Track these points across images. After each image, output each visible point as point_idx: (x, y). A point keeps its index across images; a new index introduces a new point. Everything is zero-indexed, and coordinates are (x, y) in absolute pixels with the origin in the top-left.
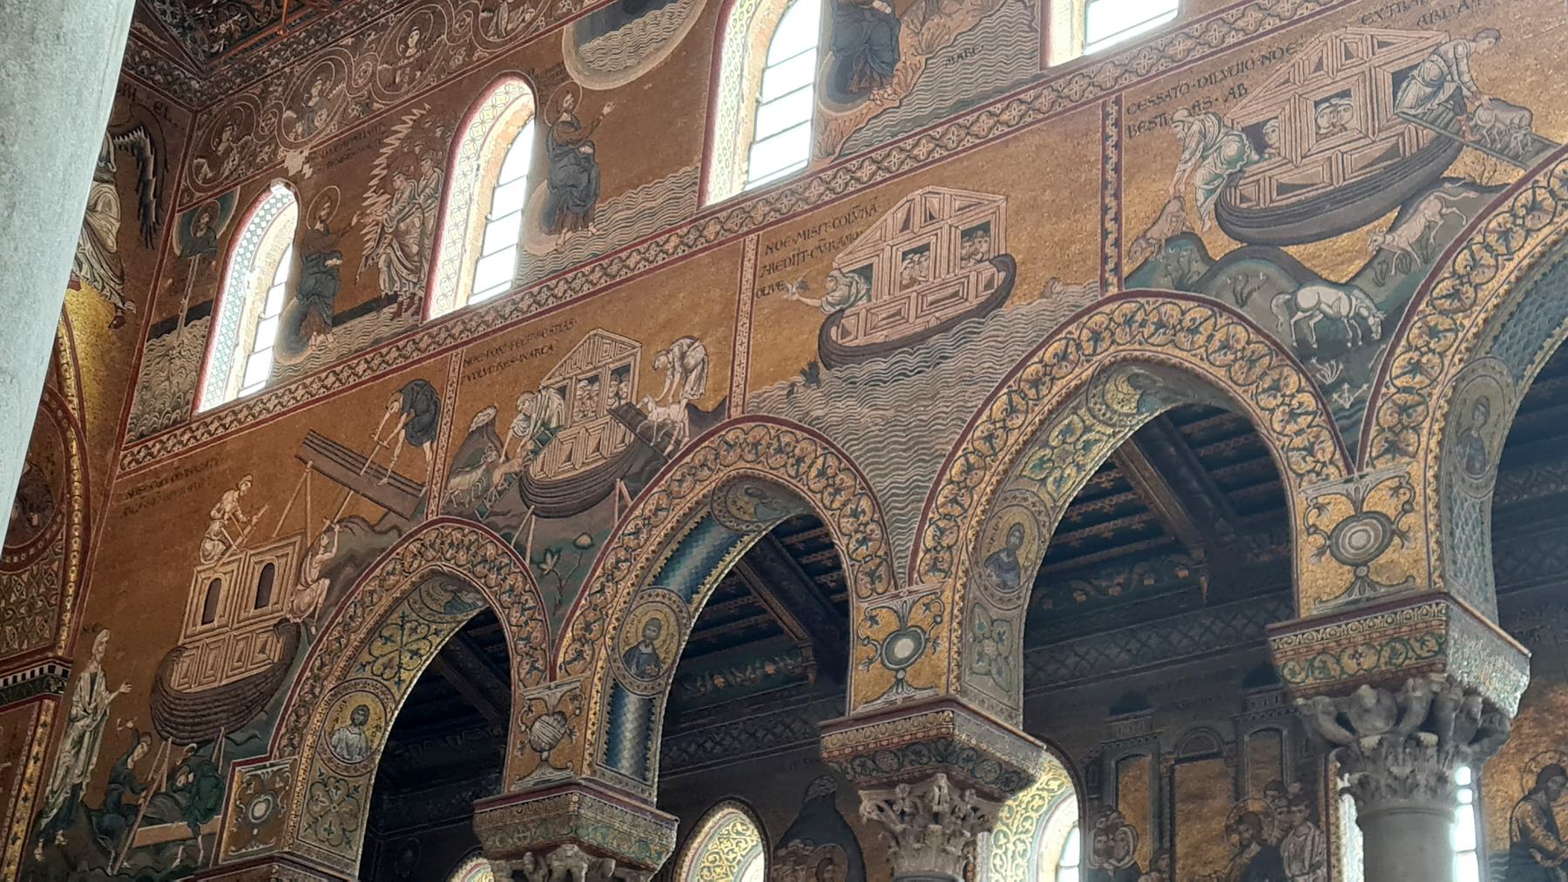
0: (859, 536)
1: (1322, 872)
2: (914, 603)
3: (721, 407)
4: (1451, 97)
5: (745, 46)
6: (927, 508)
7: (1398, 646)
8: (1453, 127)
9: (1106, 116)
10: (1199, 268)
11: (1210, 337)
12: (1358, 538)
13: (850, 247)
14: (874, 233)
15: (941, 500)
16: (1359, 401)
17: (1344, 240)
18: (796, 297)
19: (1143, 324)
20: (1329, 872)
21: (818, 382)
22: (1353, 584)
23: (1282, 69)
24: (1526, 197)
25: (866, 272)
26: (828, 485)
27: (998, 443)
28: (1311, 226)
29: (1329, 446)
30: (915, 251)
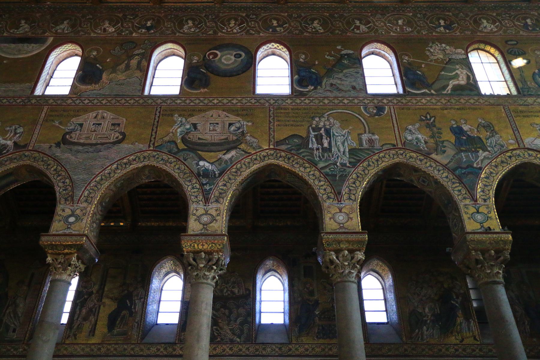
0: (64, 188)
1: (142, 300)
2: (77, 209)
3: (25, 146)
4: (241, 132)
5: (52, 62)
6: (87, 186)
7: (213, 245)
8: (241, 138)
9: (157, 110)
10: (175, 150)
11: (175, 166)
12: (205, 219)
13: (77, 118)
14: (86, 116)
15: (91, 185)
16: (211, 189)
17: (212, 154)
18: (57, 125)
19: (158, 158)
20: (144, 300)
21: (60, 147)
22: (202, 229)
23: (203, 114)
24: (255, 157)
25: (81, 125)
26: (56, 173)
27: (112, 175)
28: (206, 148)
29: (201, 197)
30: (97, 124)
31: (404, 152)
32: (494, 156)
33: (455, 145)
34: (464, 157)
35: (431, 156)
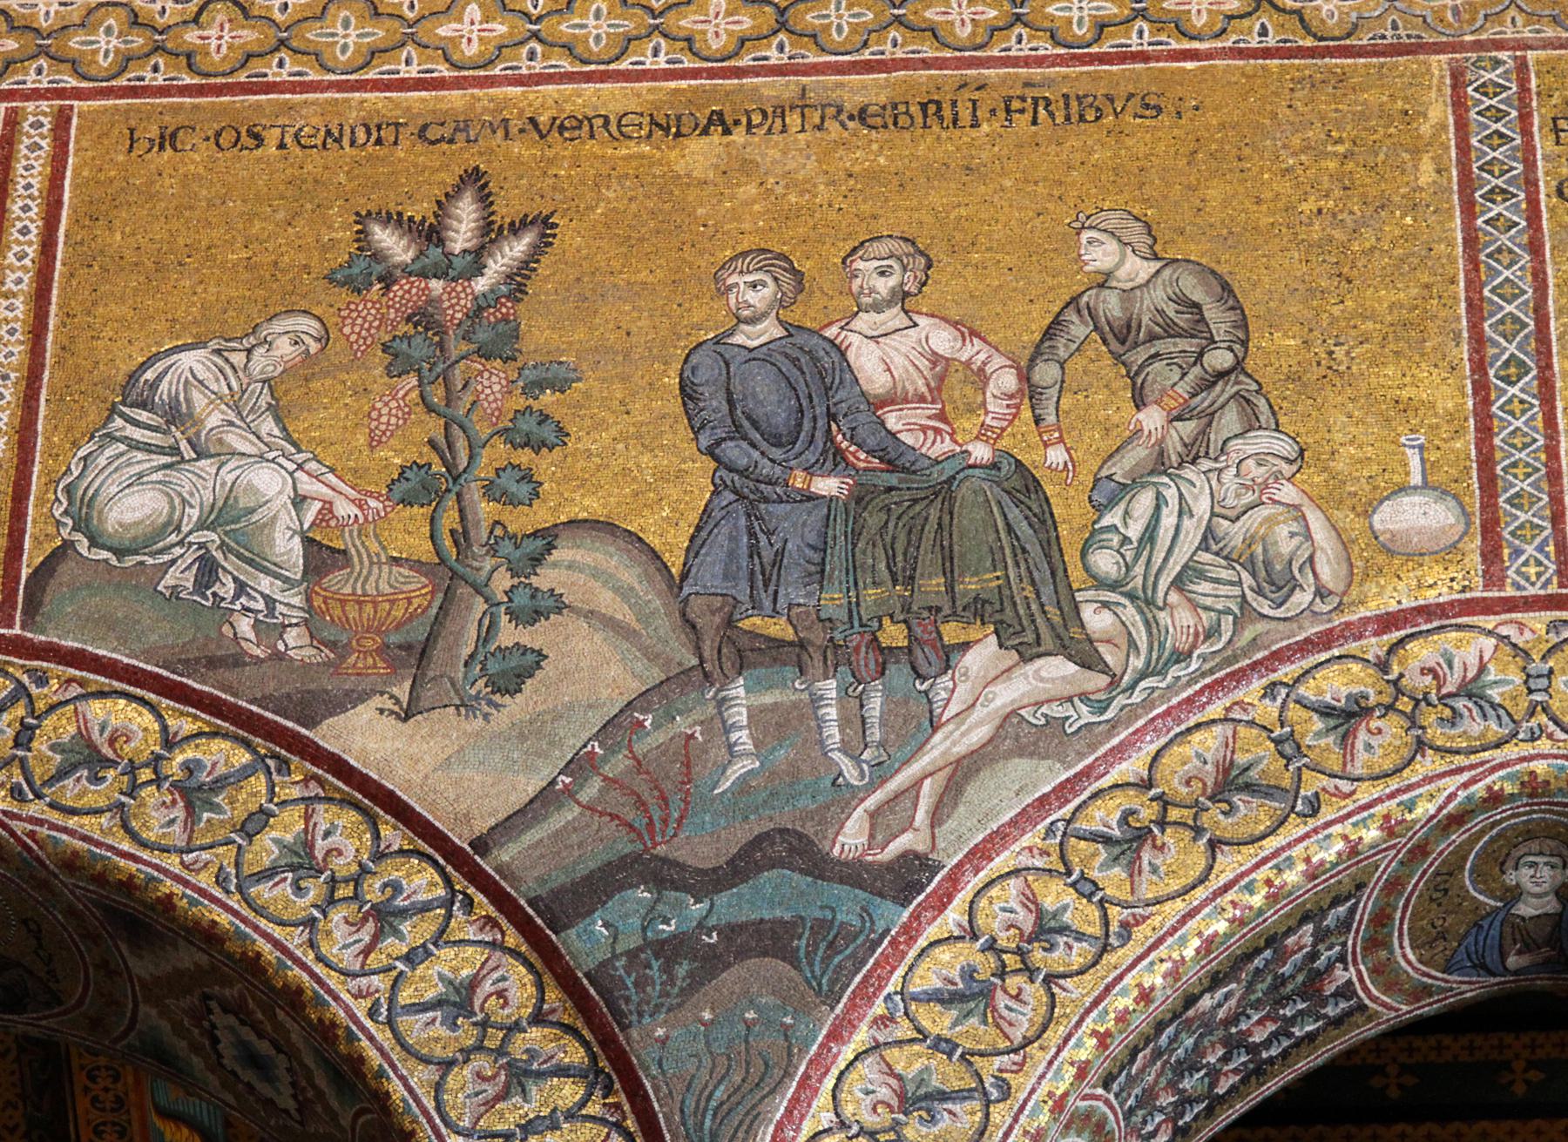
31: (20, 691)
32: (1131, 713)
33: (675, 585)
34: (742, 737)
35: (329, 735)
